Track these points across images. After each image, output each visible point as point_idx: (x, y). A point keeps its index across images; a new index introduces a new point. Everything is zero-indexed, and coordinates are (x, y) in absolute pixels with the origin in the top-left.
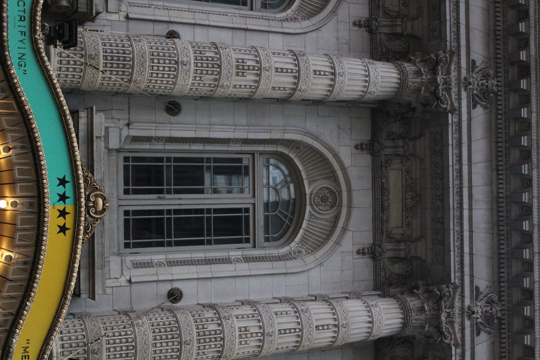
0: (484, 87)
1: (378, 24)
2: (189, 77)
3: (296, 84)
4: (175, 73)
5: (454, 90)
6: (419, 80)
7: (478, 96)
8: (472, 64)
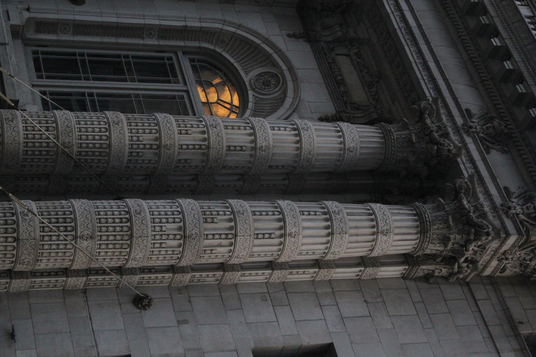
0: (491, 130)
1: (348, 115)
2: (124, 136)
3: (254, 141)
4: (107, 134)
5: (454, 137)
6: (406, 132)
7: (485, 139)
8: (467, 114)
